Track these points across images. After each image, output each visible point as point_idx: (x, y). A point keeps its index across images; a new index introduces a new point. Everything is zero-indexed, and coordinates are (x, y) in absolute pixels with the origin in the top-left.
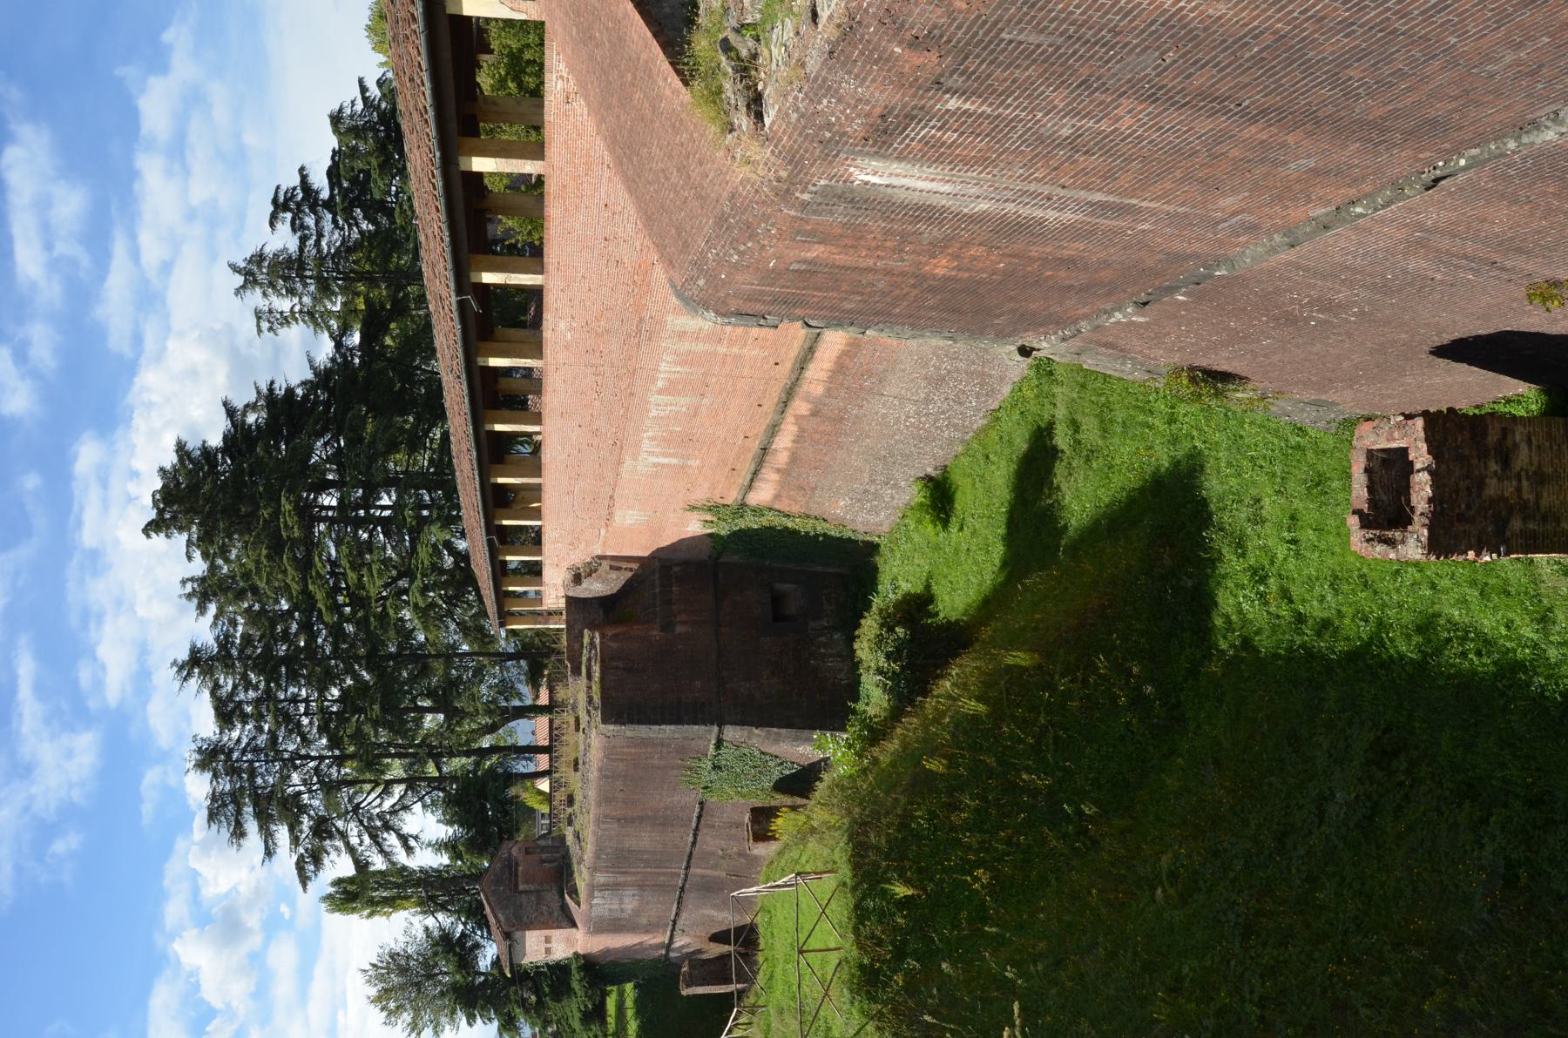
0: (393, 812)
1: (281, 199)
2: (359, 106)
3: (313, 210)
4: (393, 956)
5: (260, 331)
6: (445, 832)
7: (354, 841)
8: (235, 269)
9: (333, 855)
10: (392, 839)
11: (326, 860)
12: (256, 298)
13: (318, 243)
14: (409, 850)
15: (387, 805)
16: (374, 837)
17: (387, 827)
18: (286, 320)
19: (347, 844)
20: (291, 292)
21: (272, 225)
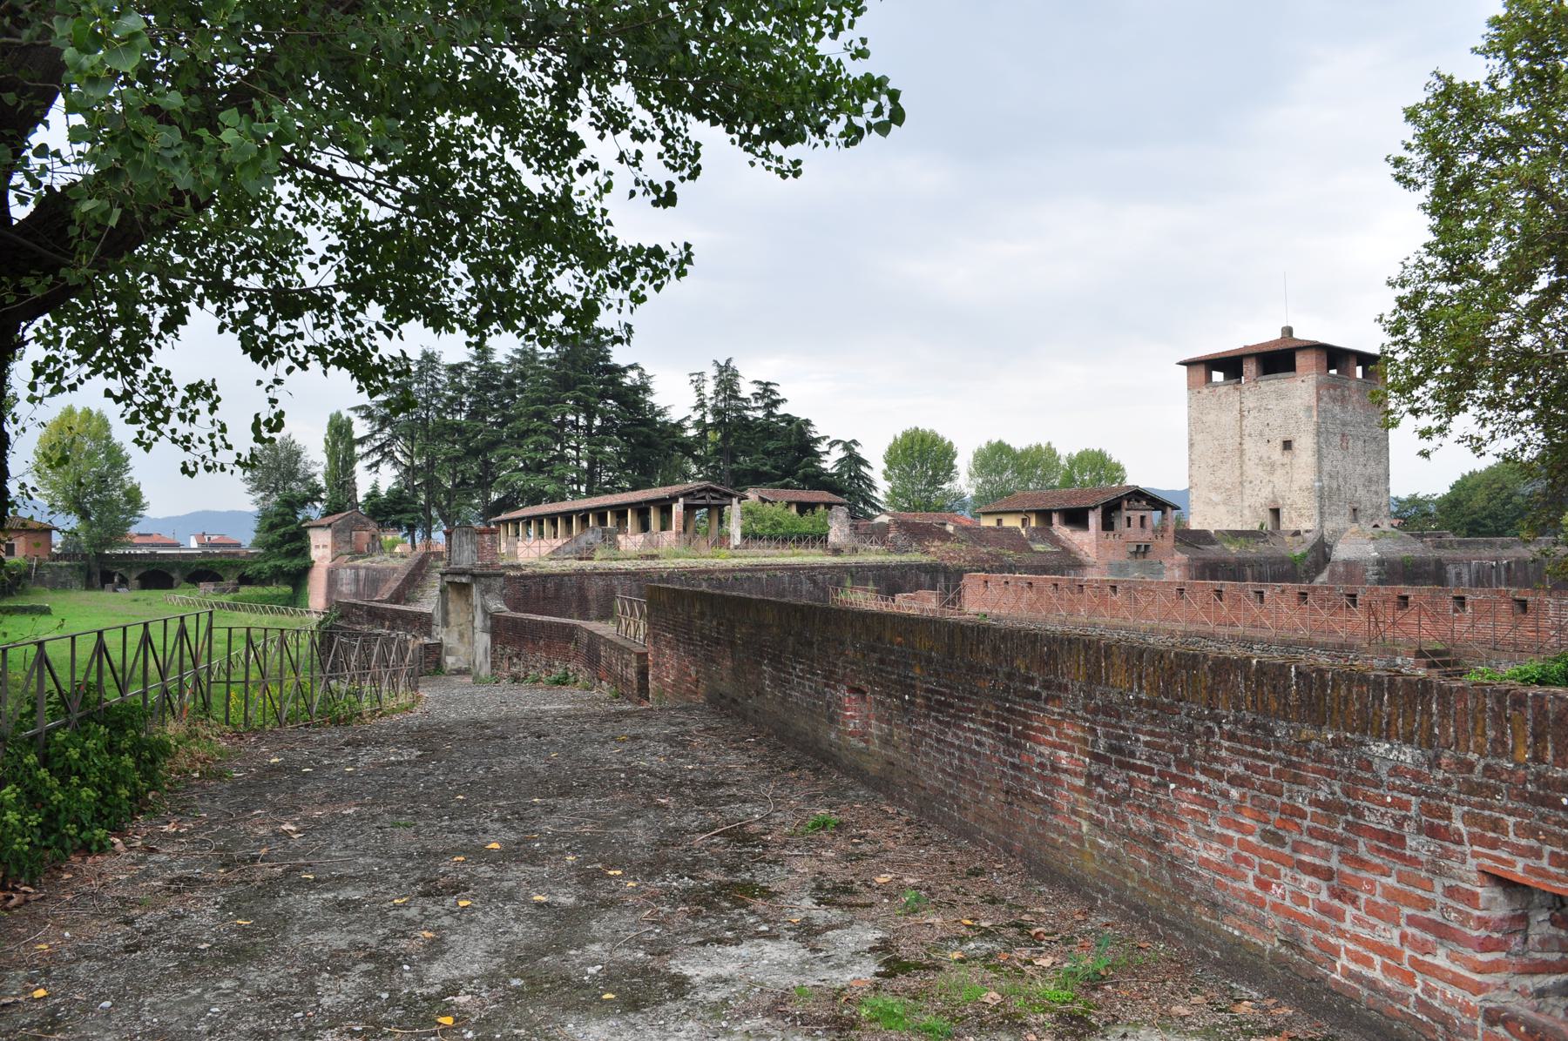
0: (393, 458)
1: (771, 387)
2: (815, 436)
3: (767, 406)
4: (298, 454)
5: (691, 375)
6: (383, 490)
7: (377, 436)
8: (729, 361)
9: (369, 425)
10: (377, 457)
11: (365, 421)
12: (712, 372)
13: (747, 408)
14: (370, 467)
15: (398, 455)
16: (378, 447)
17: (384, 455)
18: (698, 389)
19: (375, 433)
20: (717, 393)
21: (755, 382)
